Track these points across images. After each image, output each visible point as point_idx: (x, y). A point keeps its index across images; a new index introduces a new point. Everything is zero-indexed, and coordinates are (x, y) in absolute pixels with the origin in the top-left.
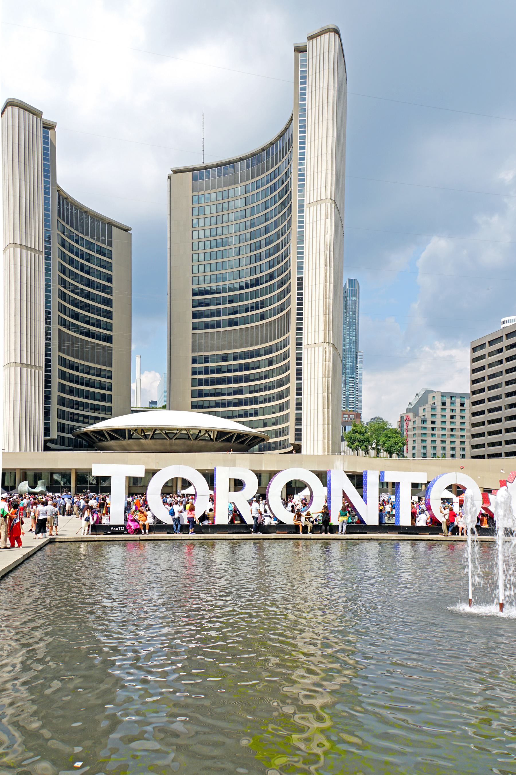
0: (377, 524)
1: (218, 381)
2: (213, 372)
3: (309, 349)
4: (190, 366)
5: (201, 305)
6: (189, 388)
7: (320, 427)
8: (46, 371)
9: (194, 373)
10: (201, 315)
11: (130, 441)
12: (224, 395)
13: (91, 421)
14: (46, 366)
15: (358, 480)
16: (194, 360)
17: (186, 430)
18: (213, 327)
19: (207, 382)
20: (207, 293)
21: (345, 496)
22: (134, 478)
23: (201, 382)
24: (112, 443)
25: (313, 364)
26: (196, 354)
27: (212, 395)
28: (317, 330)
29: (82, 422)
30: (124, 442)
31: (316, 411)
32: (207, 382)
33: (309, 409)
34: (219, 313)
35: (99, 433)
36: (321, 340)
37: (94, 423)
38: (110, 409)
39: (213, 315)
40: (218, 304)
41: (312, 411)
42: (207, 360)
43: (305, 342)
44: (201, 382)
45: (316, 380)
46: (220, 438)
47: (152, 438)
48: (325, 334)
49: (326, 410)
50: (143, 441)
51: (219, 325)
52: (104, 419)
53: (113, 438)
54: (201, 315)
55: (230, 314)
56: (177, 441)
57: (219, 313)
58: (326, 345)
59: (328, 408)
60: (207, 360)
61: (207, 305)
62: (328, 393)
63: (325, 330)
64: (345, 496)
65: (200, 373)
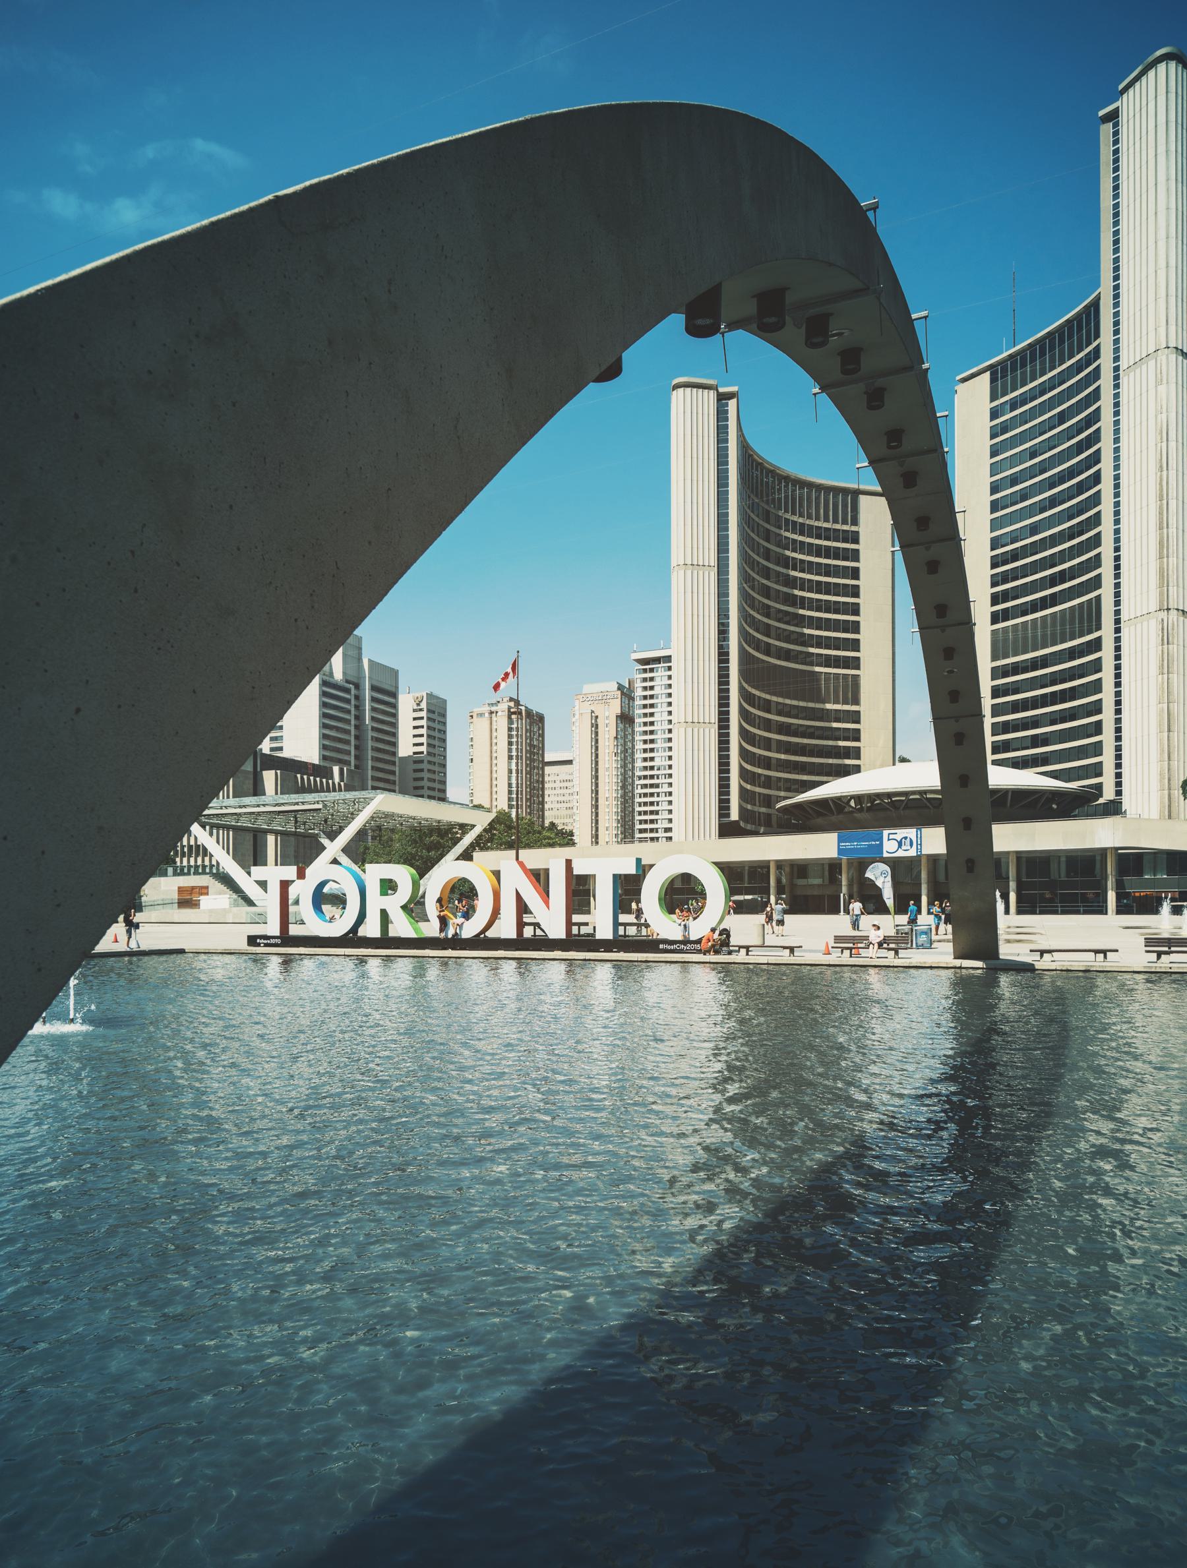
0: (515, 936)
3: (1133, 628)
8: (720, 728)
11: (841, 817)
14: (720, 720)
15: (540, 878)
19: (1016, 707)
21: (519, 897)
25: (1139, 654)
29: (788, 790)
30: (834, 818)
32: (1016, 707)
35: (799, 806)
36: (1154, 606)
38: (859, 766)
43: (1124, 616)
45: (1145, 681)
48: (1161, 594)
52: (823, 783)
63: (1161, 586)
64: (519, 897)
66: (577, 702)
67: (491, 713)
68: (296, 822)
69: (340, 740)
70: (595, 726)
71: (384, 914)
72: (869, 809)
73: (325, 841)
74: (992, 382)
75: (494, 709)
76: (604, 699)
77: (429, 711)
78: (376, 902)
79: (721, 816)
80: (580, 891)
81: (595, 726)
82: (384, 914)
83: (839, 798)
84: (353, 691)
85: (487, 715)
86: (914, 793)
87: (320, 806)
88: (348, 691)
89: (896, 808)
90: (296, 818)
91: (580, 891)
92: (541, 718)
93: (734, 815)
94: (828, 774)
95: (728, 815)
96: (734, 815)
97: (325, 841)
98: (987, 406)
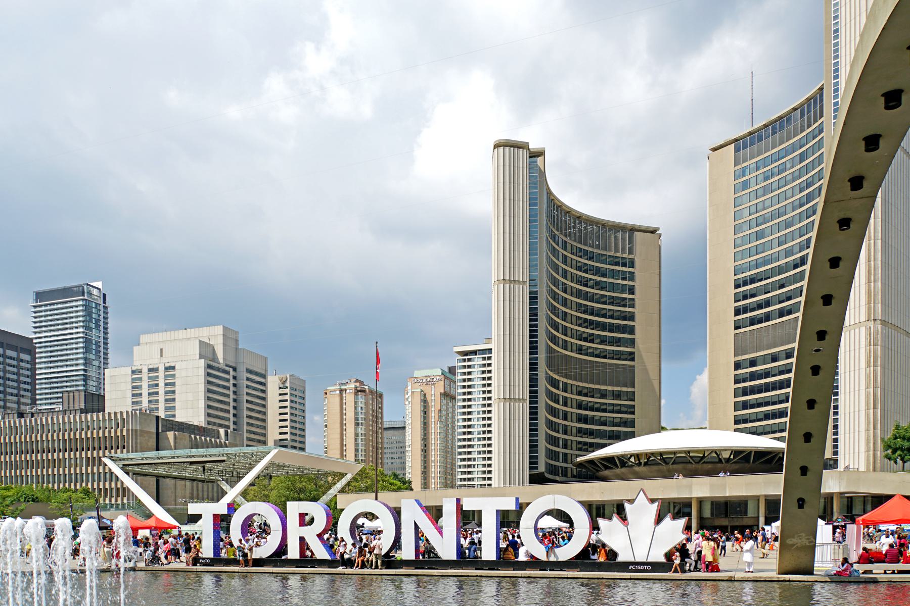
1: (767, 388)
2: (760, 377)
4: (733, 372)
5: (745, 297)
6: (731, 400)
7: (863, 434)
9: (736, 382)
10: (745, 310)
11: (624, 470)
12: (774, 403)
13: (590, 449)
16: (738, 366)
17: (685, 452)
18: (760, 321)
20: (753, 281)
21: (416, 527)
22: (503, 511)
23: (745, 392)
24: (607, 473)
26: (740, 358)
27: (759, 405)
28: (857, 305)
30: (619, 471)
31: (857, 413)
33: (847, 411)
34: (768, 303)
35: (591, 462)
37: (593, 451)
39: (760, 306)
40: (765, 293)
41: (852, 415)
42: (753, 363)
44: (745, 392)
46: (759, 459)
47: (646, 464)
49: (872, 411)
50: (637, 469)
51: (767, 317)
53: (607, 468)
54: (745, 310)
55: (780, 302)
56: (675, 466)
57: (768, 303)
58: (871, 324)
59: (875, 408)
60: (753, 363)
61: (753, 296)
62: (875, 387)
64: (416, 527)
65: (744, 381)
66: (409, 383)
67: (341, 390)
68: (204, 470)
69: (222, 410)
70: (425, 402)
71: (302, 540)
72: (646, 464)
73: (225, 486)
74: (735, 152)
75: (343, 387)
76: (430, 381)
77: (291, 388)
78: (295, 532)
79: (531, 468)
80: (468, 519)
81: (425, 402)
82: (302, 540)
83: (623, 456)
84: (232, 373)
85: (338, 392)
86: (680, 452)
87: (225, 458)
88: (228, 373)
89: (667, 463)
90: (204, 467)
91: (468, 519)
92: (381, 396)
93: (542, 468)
94: (610, 438)
95: (536, 468)
96: (542, 468)
97: (225, 486)
98: (731, 168)
